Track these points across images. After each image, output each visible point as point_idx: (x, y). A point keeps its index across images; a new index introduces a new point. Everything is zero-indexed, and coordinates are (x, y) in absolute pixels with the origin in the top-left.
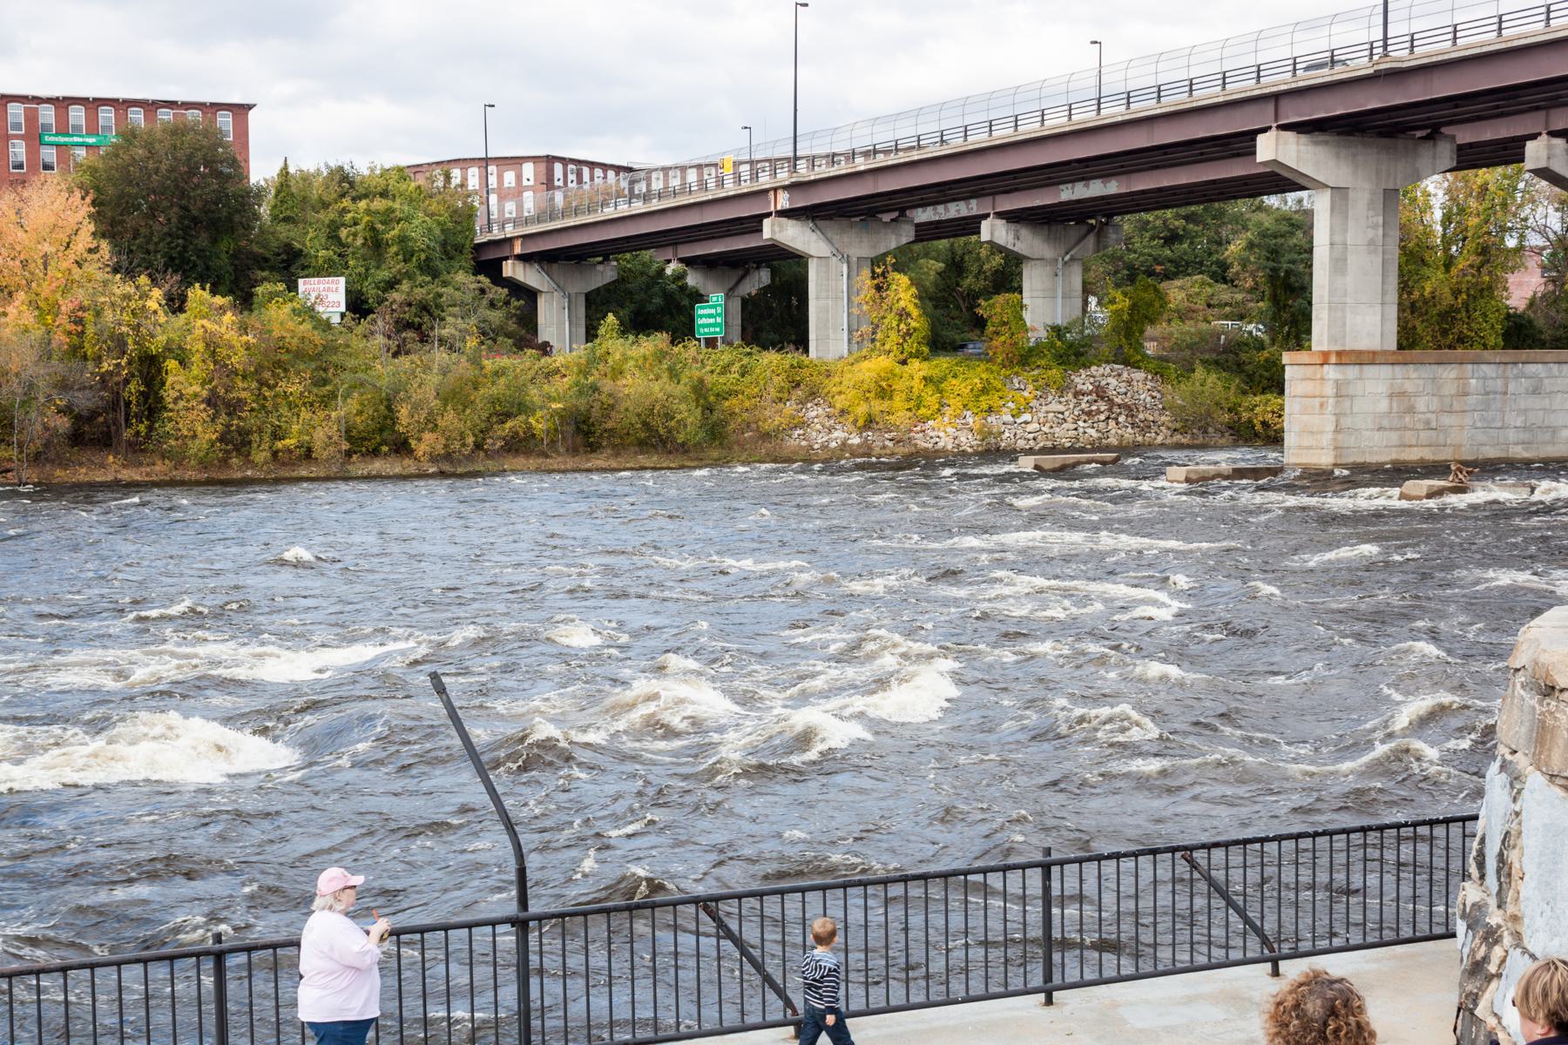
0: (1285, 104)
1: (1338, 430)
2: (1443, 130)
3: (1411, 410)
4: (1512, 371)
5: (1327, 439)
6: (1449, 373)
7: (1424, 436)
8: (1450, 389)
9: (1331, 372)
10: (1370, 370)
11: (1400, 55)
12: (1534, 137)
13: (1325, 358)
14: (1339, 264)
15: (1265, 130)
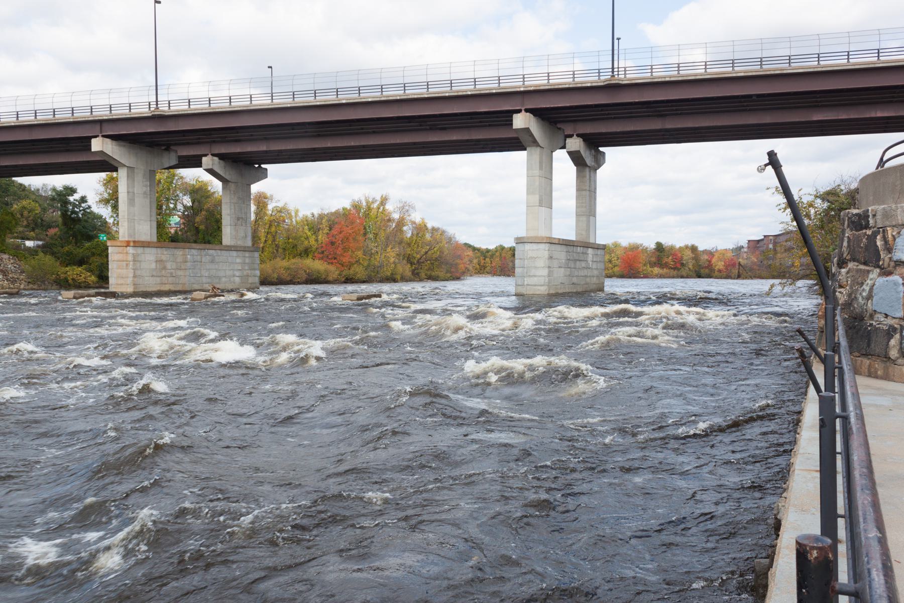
0: (105, 125)
1: (135, 277)
2: (172, 147)
3: (165, 268)
4: (203, 252)
5: (130, 280)
6: (179, 253)
7: (170, 279)
8: (180, 259)
9: (130, 250)
10: (148, 250)
11: (164, 108)
12: (206, 155)
13: (128, 244)
14: (131, 201)
15: (96, 137)
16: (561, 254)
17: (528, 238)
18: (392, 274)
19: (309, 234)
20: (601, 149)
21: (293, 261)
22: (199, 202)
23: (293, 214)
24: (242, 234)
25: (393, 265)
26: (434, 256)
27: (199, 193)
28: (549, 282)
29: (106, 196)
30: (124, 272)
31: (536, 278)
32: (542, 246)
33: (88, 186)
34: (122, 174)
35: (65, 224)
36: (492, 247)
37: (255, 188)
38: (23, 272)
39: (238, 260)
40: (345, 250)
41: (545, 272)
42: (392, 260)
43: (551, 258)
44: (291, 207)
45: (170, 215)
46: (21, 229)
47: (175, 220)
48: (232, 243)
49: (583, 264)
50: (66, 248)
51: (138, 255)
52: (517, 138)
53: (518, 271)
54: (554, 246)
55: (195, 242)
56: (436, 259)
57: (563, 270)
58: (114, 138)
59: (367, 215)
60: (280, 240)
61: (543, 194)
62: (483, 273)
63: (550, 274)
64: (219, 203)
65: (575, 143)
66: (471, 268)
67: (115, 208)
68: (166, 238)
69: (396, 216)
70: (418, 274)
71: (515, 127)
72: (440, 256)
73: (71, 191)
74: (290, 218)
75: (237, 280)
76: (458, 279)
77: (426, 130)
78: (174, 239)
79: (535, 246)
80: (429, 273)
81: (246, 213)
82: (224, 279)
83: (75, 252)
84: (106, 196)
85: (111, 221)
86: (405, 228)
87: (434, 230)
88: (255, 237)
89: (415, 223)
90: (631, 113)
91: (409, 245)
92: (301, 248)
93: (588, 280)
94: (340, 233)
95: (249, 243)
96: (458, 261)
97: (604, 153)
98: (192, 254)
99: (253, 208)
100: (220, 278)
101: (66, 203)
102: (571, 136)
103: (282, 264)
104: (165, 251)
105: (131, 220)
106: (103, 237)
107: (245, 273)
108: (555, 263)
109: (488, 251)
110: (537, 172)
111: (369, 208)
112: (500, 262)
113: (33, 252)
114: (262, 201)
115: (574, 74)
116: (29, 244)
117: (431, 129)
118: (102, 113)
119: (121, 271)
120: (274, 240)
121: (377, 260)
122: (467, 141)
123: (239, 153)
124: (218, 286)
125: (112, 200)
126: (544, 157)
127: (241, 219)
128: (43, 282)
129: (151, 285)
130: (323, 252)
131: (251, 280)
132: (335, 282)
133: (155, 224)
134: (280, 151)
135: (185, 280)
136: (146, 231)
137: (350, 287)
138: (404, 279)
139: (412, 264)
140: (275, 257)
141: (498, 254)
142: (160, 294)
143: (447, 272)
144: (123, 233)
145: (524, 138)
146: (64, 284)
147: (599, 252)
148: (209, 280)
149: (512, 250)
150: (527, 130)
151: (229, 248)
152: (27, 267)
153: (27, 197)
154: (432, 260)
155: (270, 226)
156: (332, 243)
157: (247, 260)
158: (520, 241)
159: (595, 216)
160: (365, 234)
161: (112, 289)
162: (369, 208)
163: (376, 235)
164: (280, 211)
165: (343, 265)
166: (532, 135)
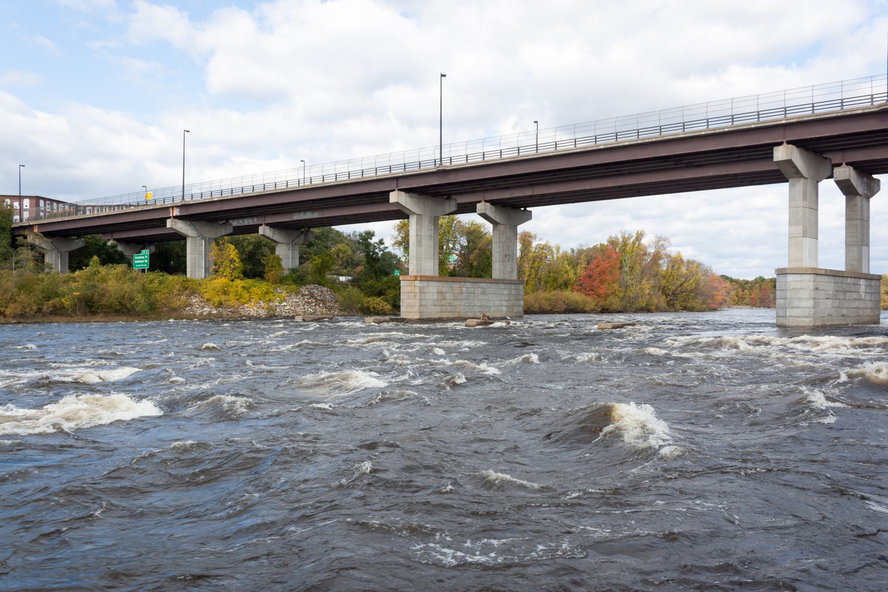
0: (400, 181)
1: (420, 305)
2: (453, 197)
3: (444, 299)
4: (476, 285)
5: (417, 309)
6: (456, 285)
7: (449, 308)
8: (457, 291)
9: (418, 283)
10: (431, 283)
11: (446, 164)
12: (480, 202)
13: (416, 278)
14: (419, 243)
15: (393, 191)
16: (828, 285)
17: (791, 269)
18: (647, 305)
19: (568, 268)
20: (875, 176)
21: (554, 292)
22: (473, 242)
23: (555, 251)
24: (509, 269)
25: (648, 297)
26: (689, 288)
27: (473, 234)
28: (815, 313)
29: (399, 239)
30: (412, 302)
31: (799, 310)
32: (807, 277)
33: (384, 232)
34: (413, 220)
35: (368, 263)
36: (751, 278)
37: (521, 228)
38: (337, 301)
39: (506, 292)
40: (602, 282)
41: (810, 303)
42: (647, 291)
43: (817, 289)
44: (553, 244)
45: (450, 254)
46: (337, 267)
47: (454, 258)
48: (501, 277)
49: (855, 296)
50: (369, 282)
51: (424, 287)
52: (779, 171)
53: (779, 302)
54: (819, 278)
55: (470, 276)
56: (692, 291)
57: (830, 301)
58: (407, 191)
59: (623, 250)
60: (543, 274)
61: (807, 224)
62: (742, 304)
63: (815, 306)
64: (490, 243)
65: (845, 172)
66: (728, 299)
67: (406, 249)
68: (447, 274)
69: (652, 250)
70: (673, 305)
71: (776, 159)
72: (696, 288)
73: (370, 235)
74: (552, 253)
75: (504, 309)
76: (715, 310)
77: (681, 168)
78: (453, 274)
79: (798, 277)
80: (684, 304)
81: (513, 251)
82: (493, 309)
83: (375, 286)
84: (399, 239)
85: (403, 259)
86: (661, 262)
87: (690, 263)
88: (520, 272)
89: (670, 256)
90: (880, 140)
91: (664, 277)
92: (560, 281)
93: (860, 312)
94: (598, 266)
95: (515, 276)
96: (715, 293)
97: (878, 181)
98: (467, 287)
99: (519, 246)
100: (489, 307)
101: (368, 245)
102: (839, 165)
103: (544, 296)
104: (445, 284)
105: (419, 259)
106: (397, 273)
107: (511, 303)
108: (822, 295)
109: (747, 282)
110: (800, 203)
111: (625, 244)
112: (760, 293)
113: (344, 285)
114: (527, 239)
115: (813, 107)
116: (342, 279)
117: (687, 167)
118: (398, 172)
119: (411, 302)
120: (537, 274)
121: (633, 291)
122: (724, 176)
123: (508, 199)
124: (487, 314)
125: (404, 243)
126: (808, 188)
127: (508, 256)
128: (351, 309)
129: (433, 312)
130: (581, 285)
131: (516, 309)
132: (593, 311)
133: (437, 263)
134: (543, 195)
135: (461, 309)
136: (430, 267)
137: (605, 317)
138: (659, 310)
139: (667, 295)
140: (538, 289)
141: (757, 285)
142: (440, 320)
143: (704, 303)
144: (413, 269)
145: (785, 170)
146: (366, 311)
147: (873, 283)
148: (481, 309)
149: (773, 281)
150: (789, 162)
151: (497, 282)
152: (340, 298)
153: (341, 242)
154: (684, 291)
155: (534, 262)
156: (590, 276)
157: (513, 292)
158: (781, 272)
159: (868, 245)
160: (621, 268)
161: (403, 316)
162: (625, 244)
163: (632, 268)
164: (543, 249)
165: (599, 296)
166: (795, 167)
